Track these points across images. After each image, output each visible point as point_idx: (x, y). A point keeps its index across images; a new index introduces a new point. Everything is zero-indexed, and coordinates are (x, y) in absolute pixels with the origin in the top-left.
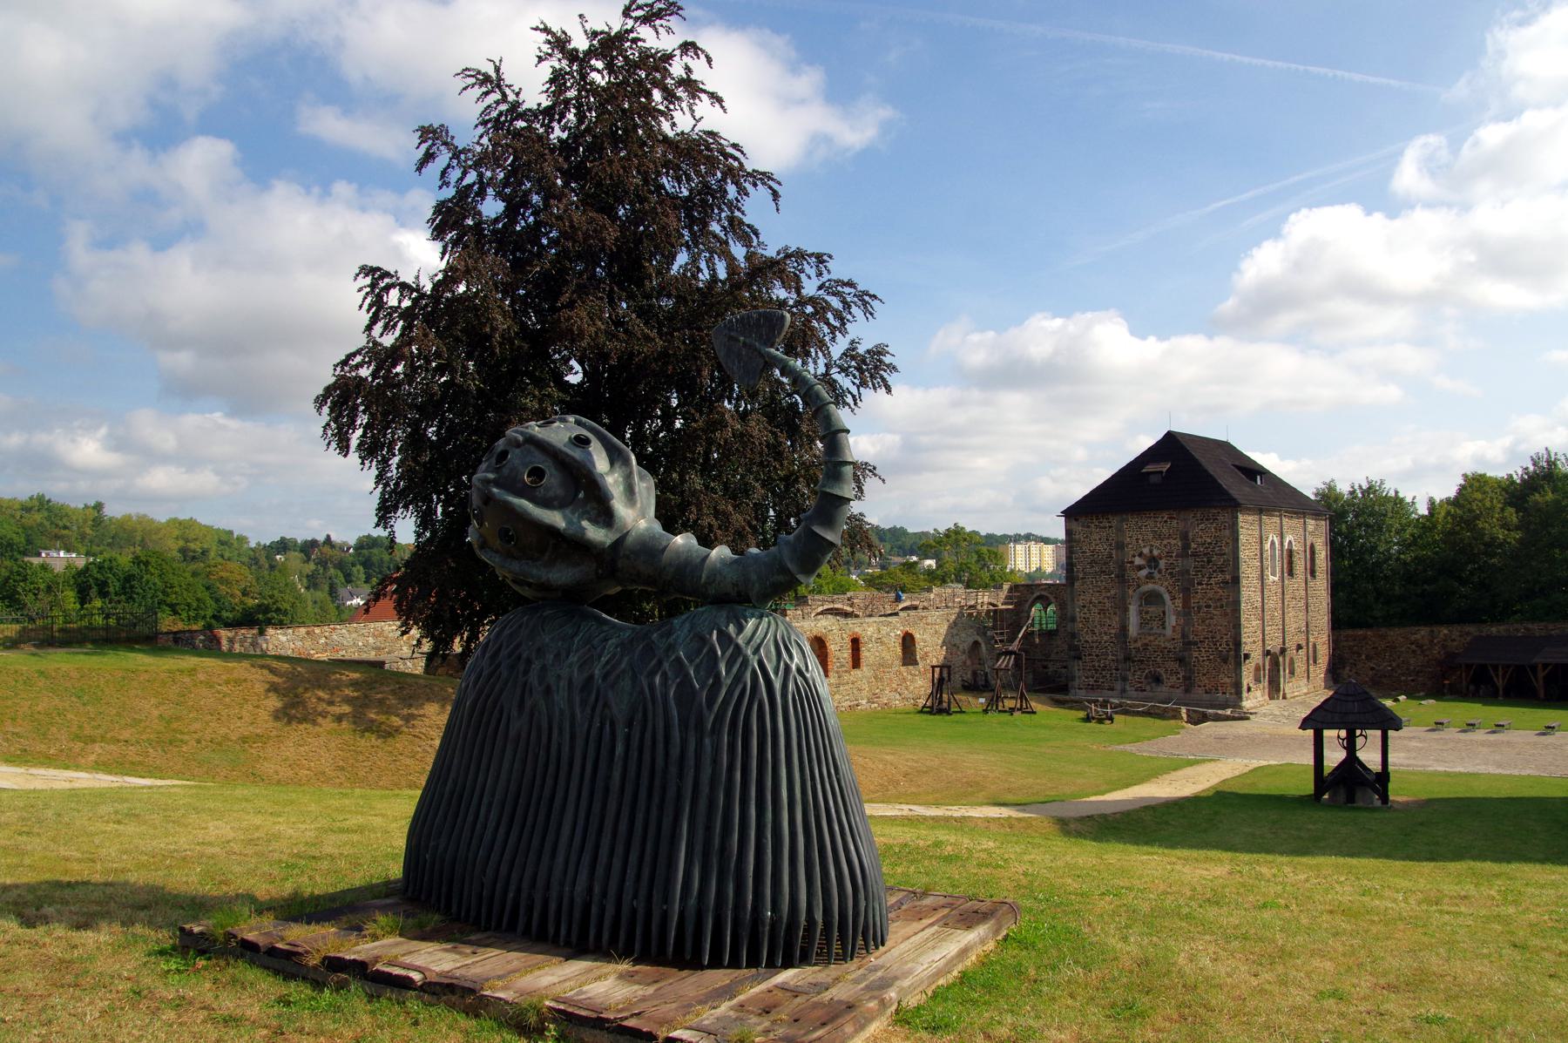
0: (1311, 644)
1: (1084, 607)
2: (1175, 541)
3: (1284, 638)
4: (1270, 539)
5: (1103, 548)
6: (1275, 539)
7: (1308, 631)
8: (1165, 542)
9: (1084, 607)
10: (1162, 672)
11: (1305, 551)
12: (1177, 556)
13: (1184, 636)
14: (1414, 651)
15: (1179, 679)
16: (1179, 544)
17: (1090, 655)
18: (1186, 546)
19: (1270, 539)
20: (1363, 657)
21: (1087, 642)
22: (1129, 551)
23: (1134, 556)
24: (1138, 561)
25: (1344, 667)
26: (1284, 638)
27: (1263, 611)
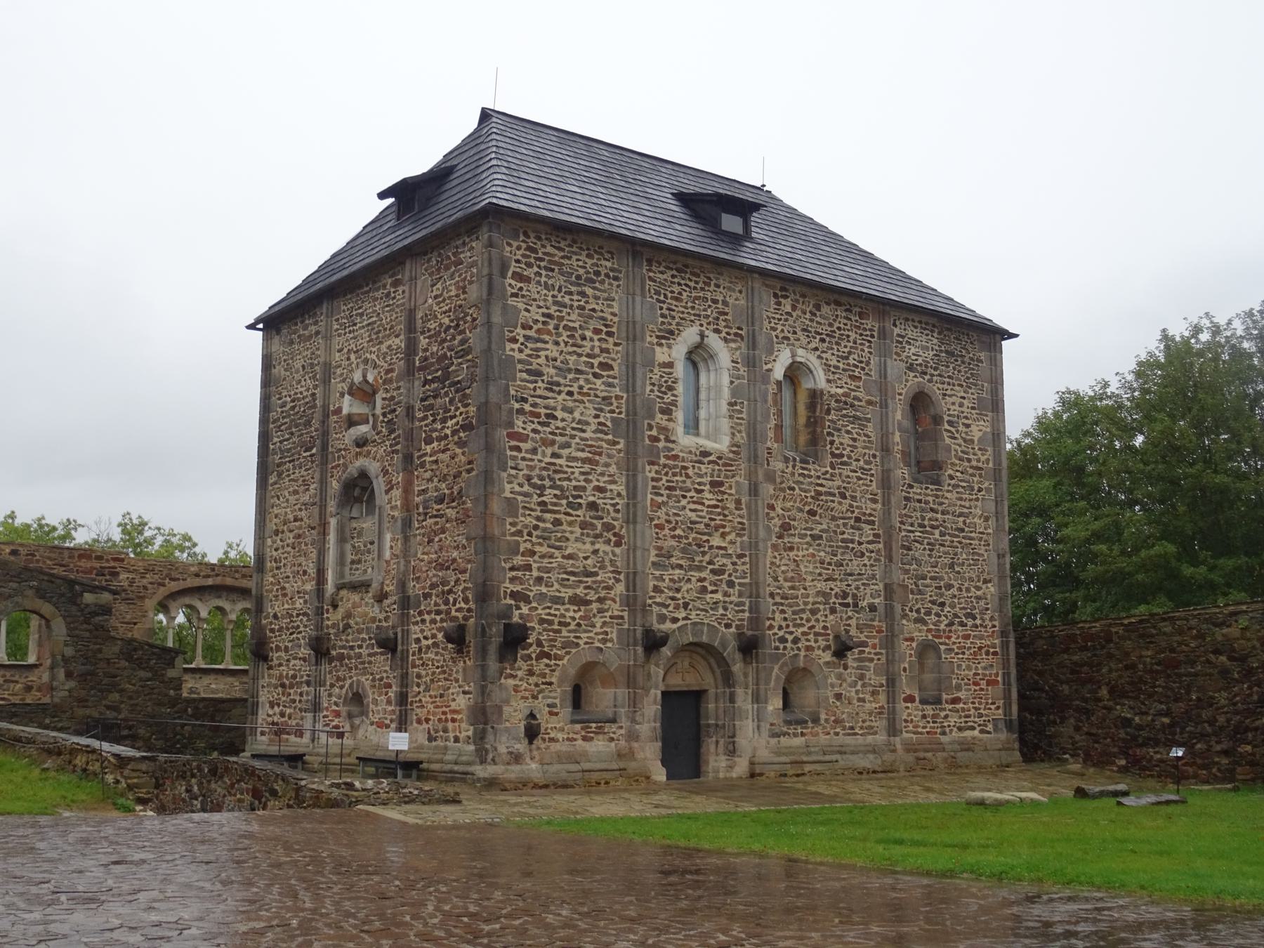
0: (906, 650)
1: (277, 533)
2: (397, 341)
3: (754, 608)
4: (690, 335)
5: (305, 386)
6: (714, 341)
7: (889, 611)
8: (384, 348)
9: (277, 533)
10: (367, 684)
11: (884, 405)
12: (399, 379)
13: (402, 585)
14: (1225, 672)
15: (389, 702)
16: (403, 346)
17: (278, 649)
18: (411, 348)
19: (690, 335)
20: (1104, 692)
21: (275, 616)
22: (338, 385)
23: (342, 395)
24: (348, 405)
25: (1063, 719)
26: (754, 608)
27: (631, 520)
